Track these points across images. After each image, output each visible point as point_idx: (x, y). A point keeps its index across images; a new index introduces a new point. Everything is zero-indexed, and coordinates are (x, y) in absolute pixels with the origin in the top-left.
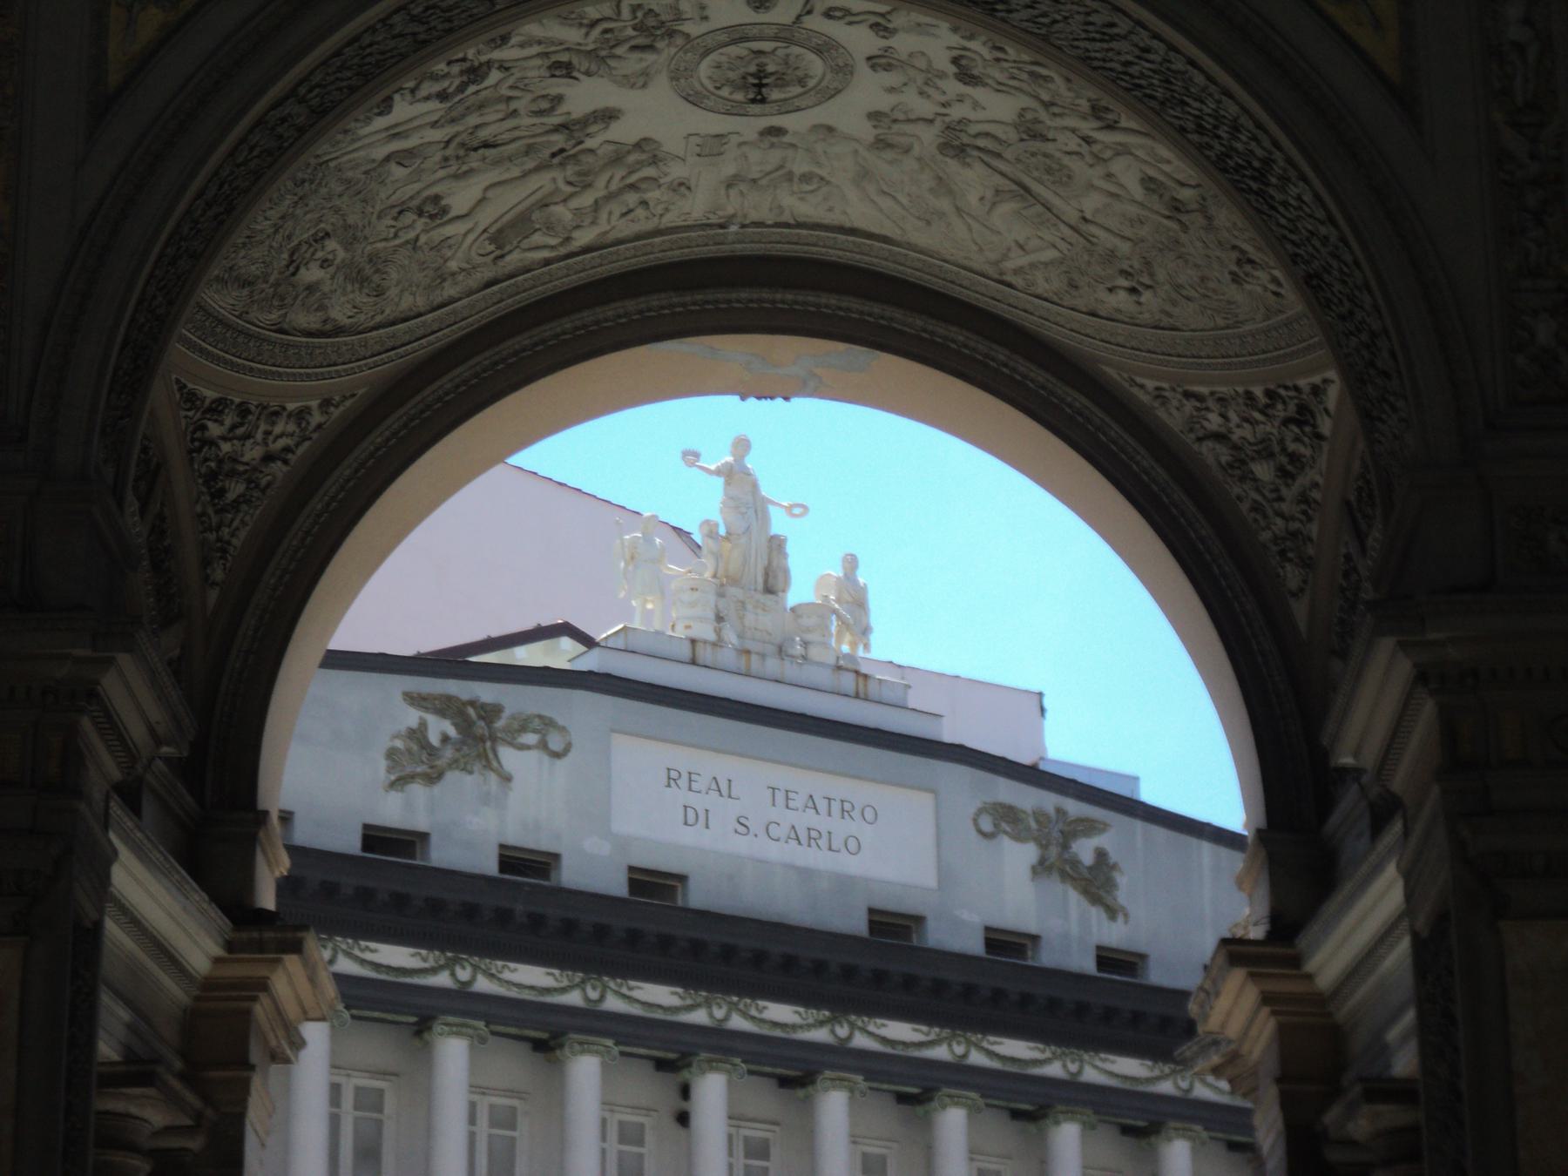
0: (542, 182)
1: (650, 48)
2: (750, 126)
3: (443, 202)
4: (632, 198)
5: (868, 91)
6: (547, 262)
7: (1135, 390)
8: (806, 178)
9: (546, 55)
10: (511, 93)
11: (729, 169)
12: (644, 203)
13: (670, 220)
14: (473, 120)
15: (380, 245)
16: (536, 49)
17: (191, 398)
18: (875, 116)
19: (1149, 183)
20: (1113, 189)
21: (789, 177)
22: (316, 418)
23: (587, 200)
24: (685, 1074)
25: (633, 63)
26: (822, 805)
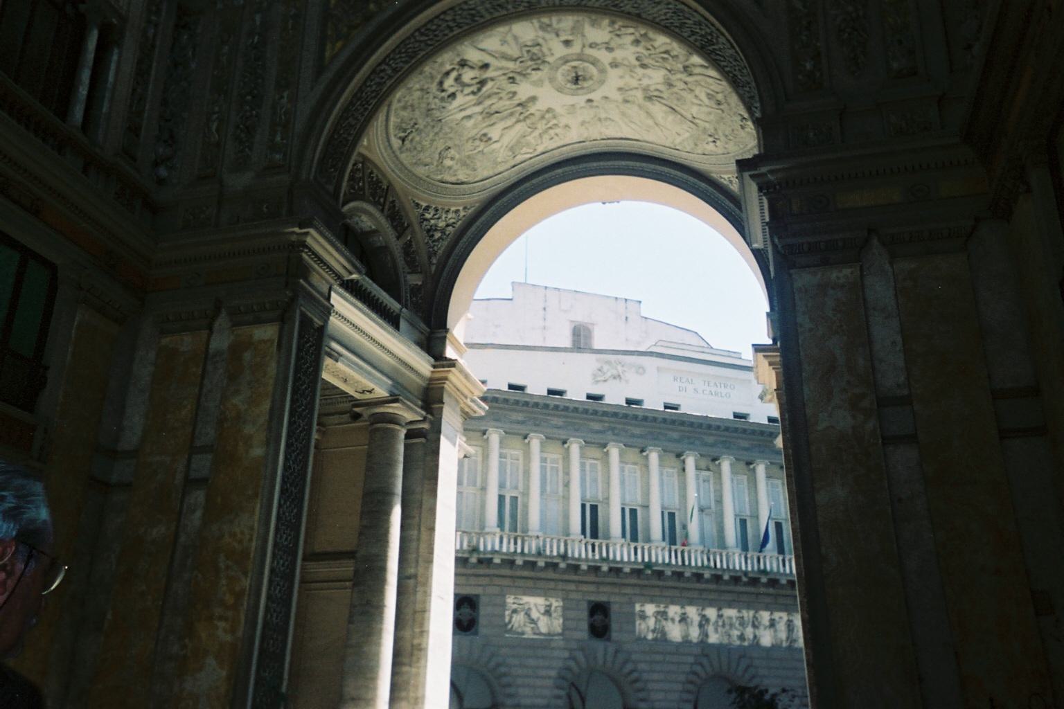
0: (521, 127)
1: (538, 69)
2: (580, 100)
3: (489, 136)
4: (552, 132)
5: (615, 79)
6: (531, 158)
7: (722, 180)
8: (606, 119)
9: (504, 74)
11: (580, 119)
12: (557, 135)
13: (567, 141)
14: (488, 103)
15: (471, 153)
16: (501, 72)
17: (418, 205)
18: (620, 89)
19: (710, 96)
20: (700, 102)
21: (600, 120)
22: (462, 214)
23: (536, 133)
24: (682, 458)
25: (536, 76)
26: (718, 385)
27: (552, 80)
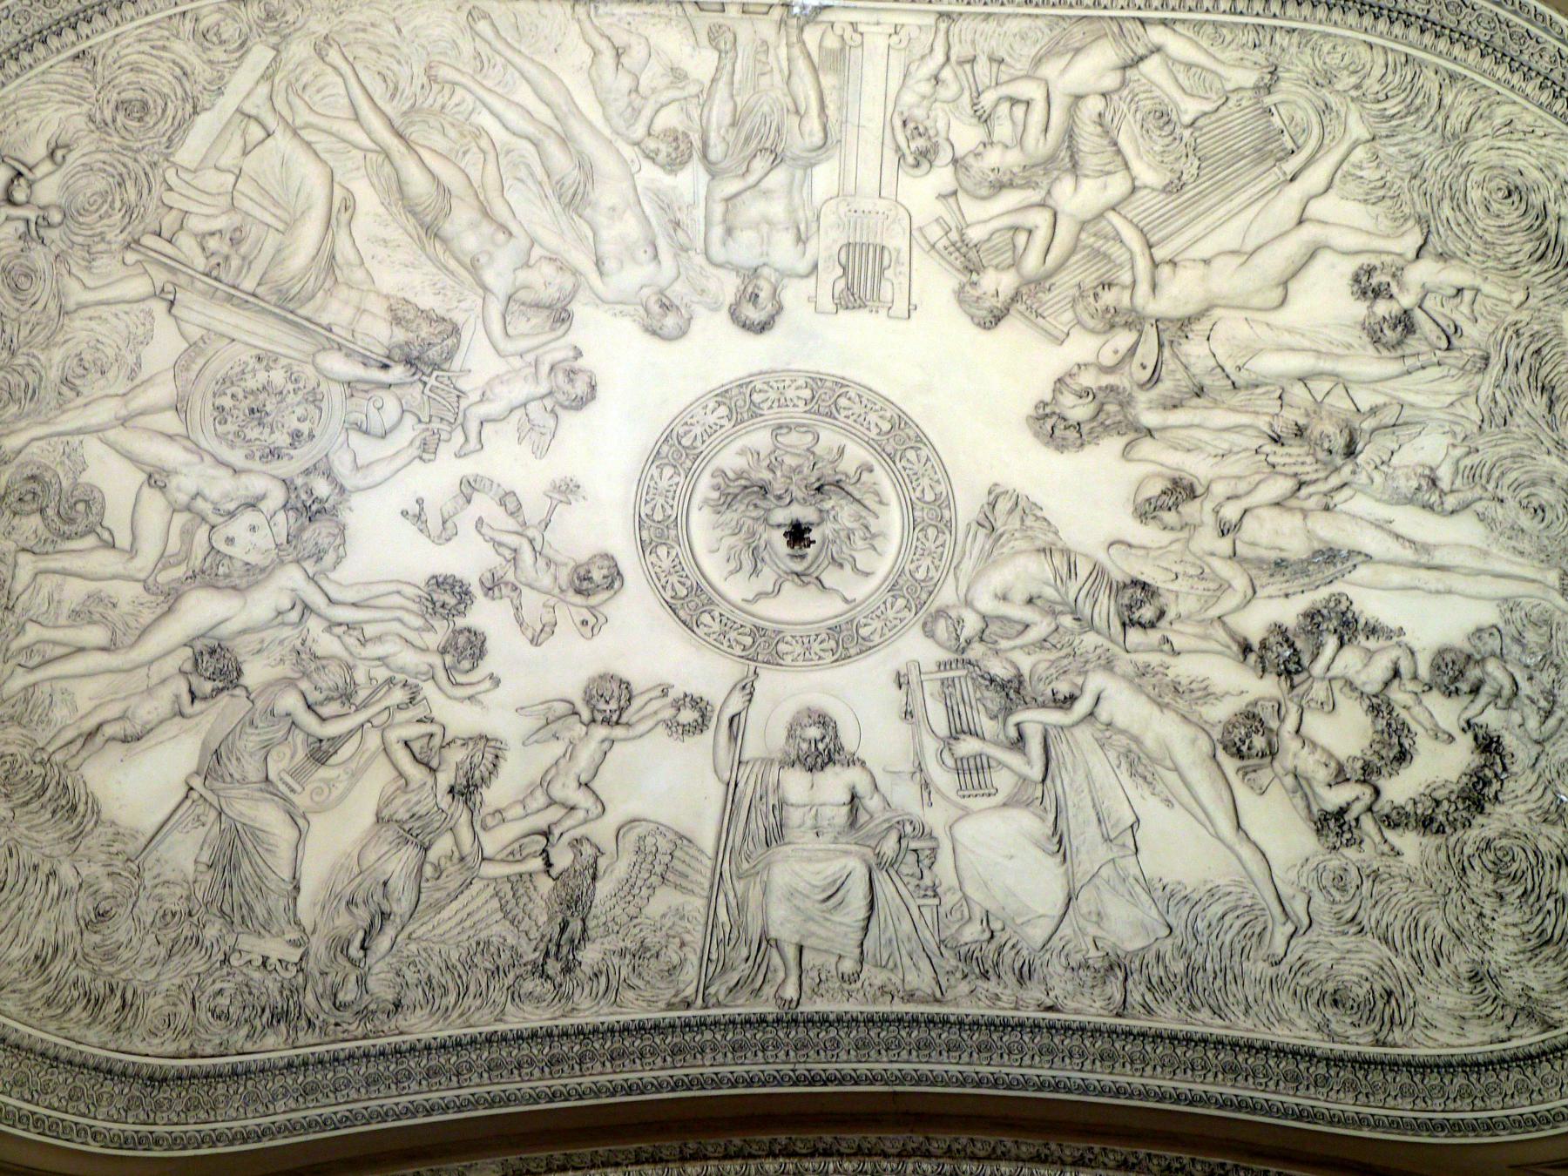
10: (1226, 570)
16: (1185, 669)
27: (930, 516)
